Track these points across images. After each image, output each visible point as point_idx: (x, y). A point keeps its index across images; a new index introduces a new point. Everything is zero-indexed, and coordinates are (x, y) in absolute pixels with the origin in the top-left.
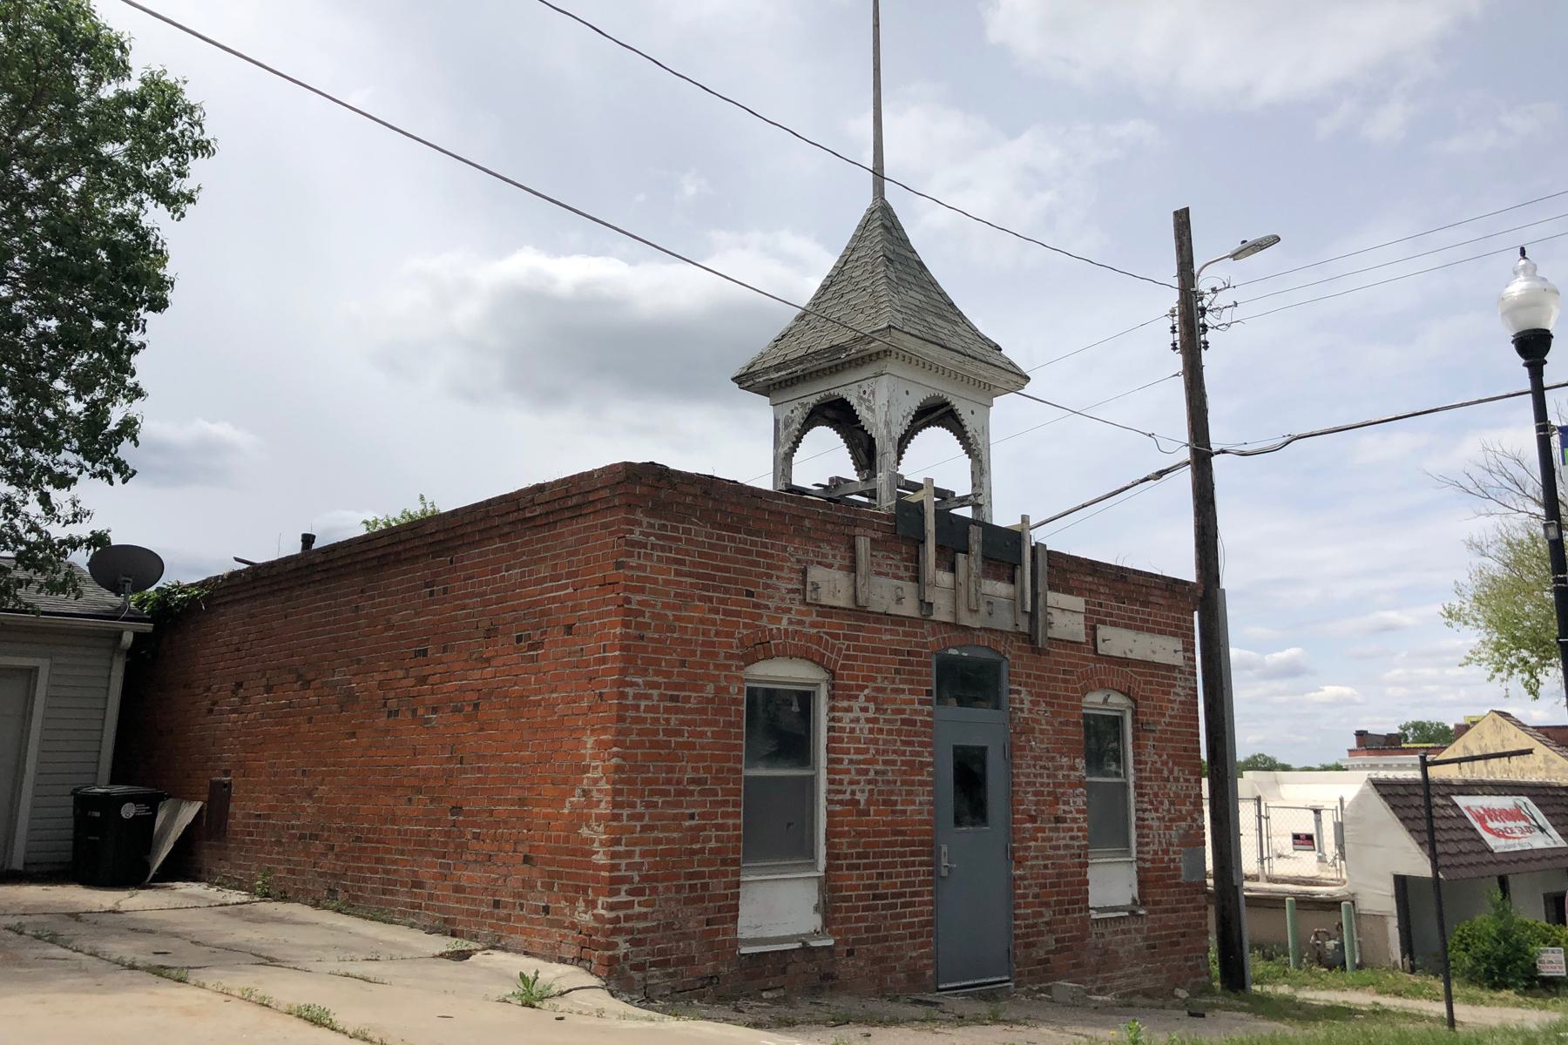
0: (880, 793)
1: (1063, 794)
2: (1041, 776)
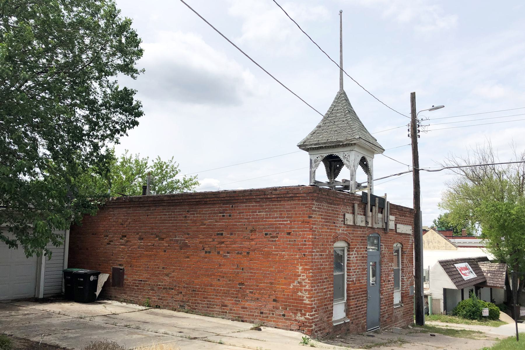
1: (390, 274)
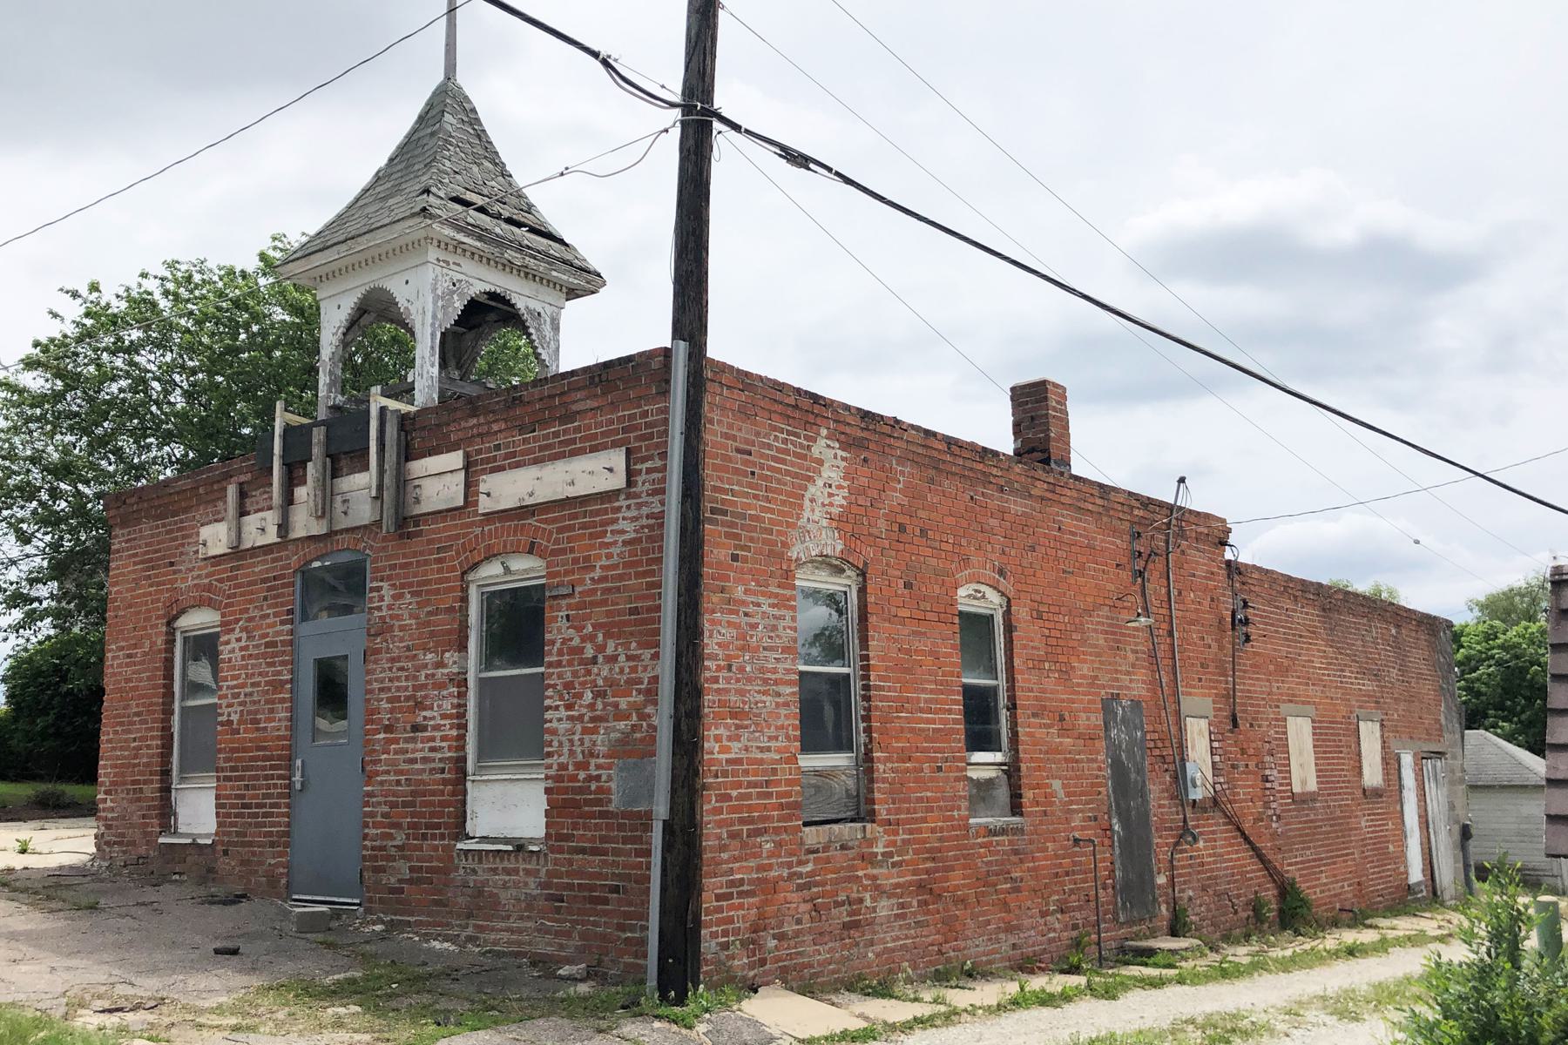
0: (249, 712)
1: (426, 697)
2: (398, 679)
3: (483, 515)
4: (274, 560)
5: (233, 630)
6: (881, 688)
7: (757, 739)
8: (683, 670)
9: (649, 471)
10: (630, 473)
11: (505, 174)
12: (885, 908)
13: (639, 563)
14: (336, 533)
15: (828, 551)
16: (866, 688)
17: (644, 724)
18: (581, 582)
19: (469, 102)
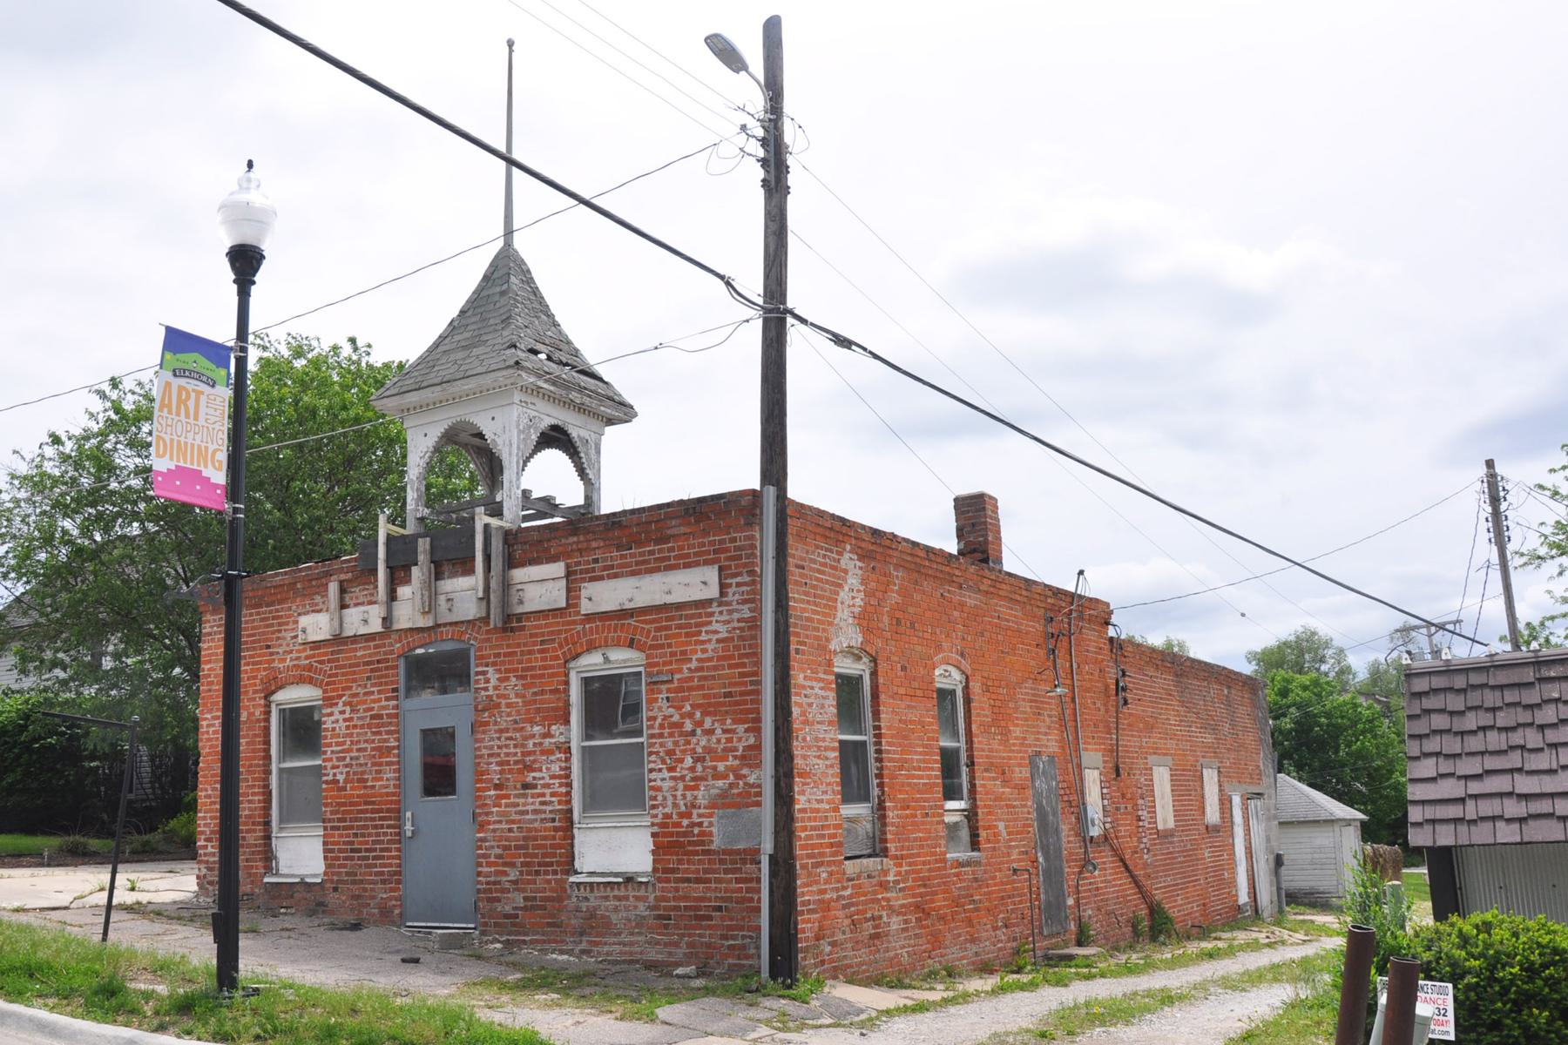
0: (354, 773)
1: (534, 761)
2: (507, 746)
3: (585, 615)
4: (376, 647)
5: (337, 704)
6: (888, 752)
7: (815, 793)
8: (780, 741)
9: (738, 585)
10: (723, 587)
11: (556, 325)
12: (895, 923)
13: (732, 657)
14: (439, 626)
15: (853, 643)
16: (879, 751)
17: (741, 783)
18: (680, 671)
19: (525, 264)
